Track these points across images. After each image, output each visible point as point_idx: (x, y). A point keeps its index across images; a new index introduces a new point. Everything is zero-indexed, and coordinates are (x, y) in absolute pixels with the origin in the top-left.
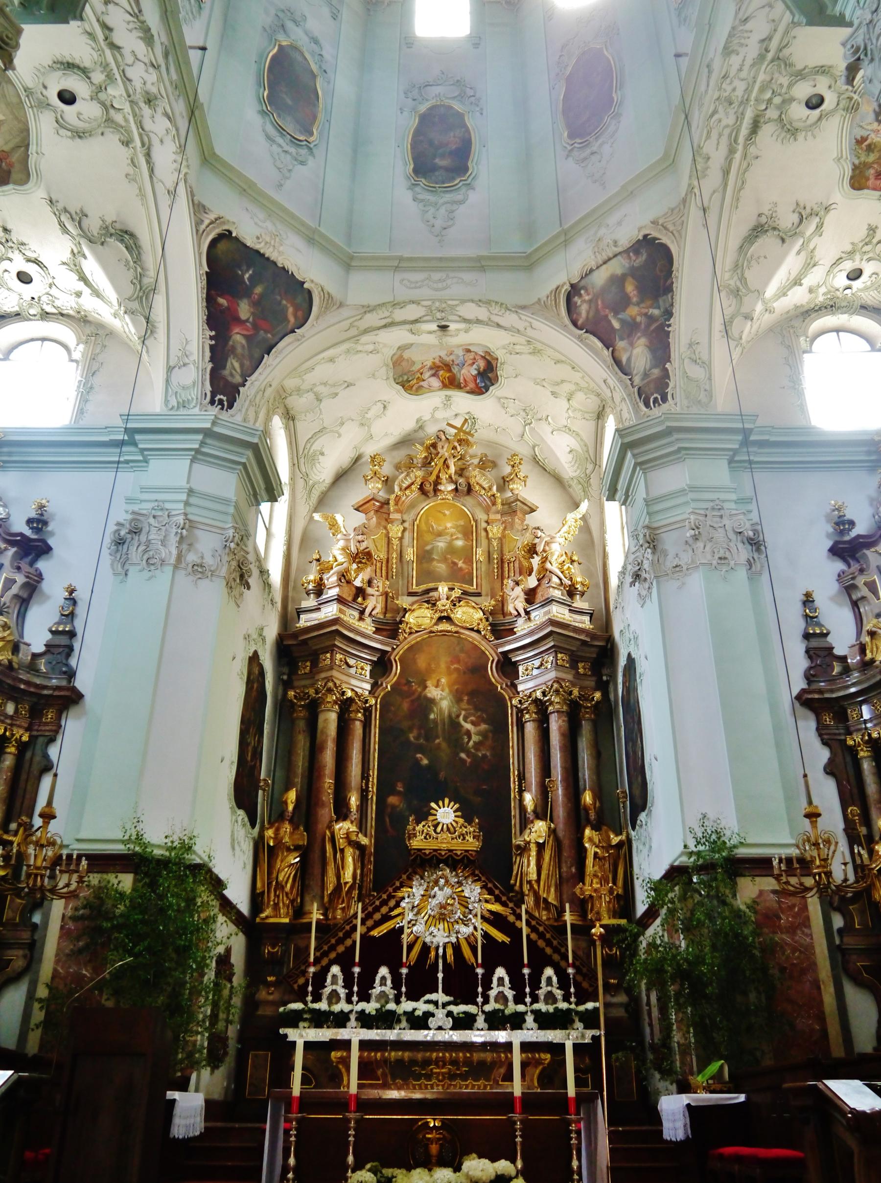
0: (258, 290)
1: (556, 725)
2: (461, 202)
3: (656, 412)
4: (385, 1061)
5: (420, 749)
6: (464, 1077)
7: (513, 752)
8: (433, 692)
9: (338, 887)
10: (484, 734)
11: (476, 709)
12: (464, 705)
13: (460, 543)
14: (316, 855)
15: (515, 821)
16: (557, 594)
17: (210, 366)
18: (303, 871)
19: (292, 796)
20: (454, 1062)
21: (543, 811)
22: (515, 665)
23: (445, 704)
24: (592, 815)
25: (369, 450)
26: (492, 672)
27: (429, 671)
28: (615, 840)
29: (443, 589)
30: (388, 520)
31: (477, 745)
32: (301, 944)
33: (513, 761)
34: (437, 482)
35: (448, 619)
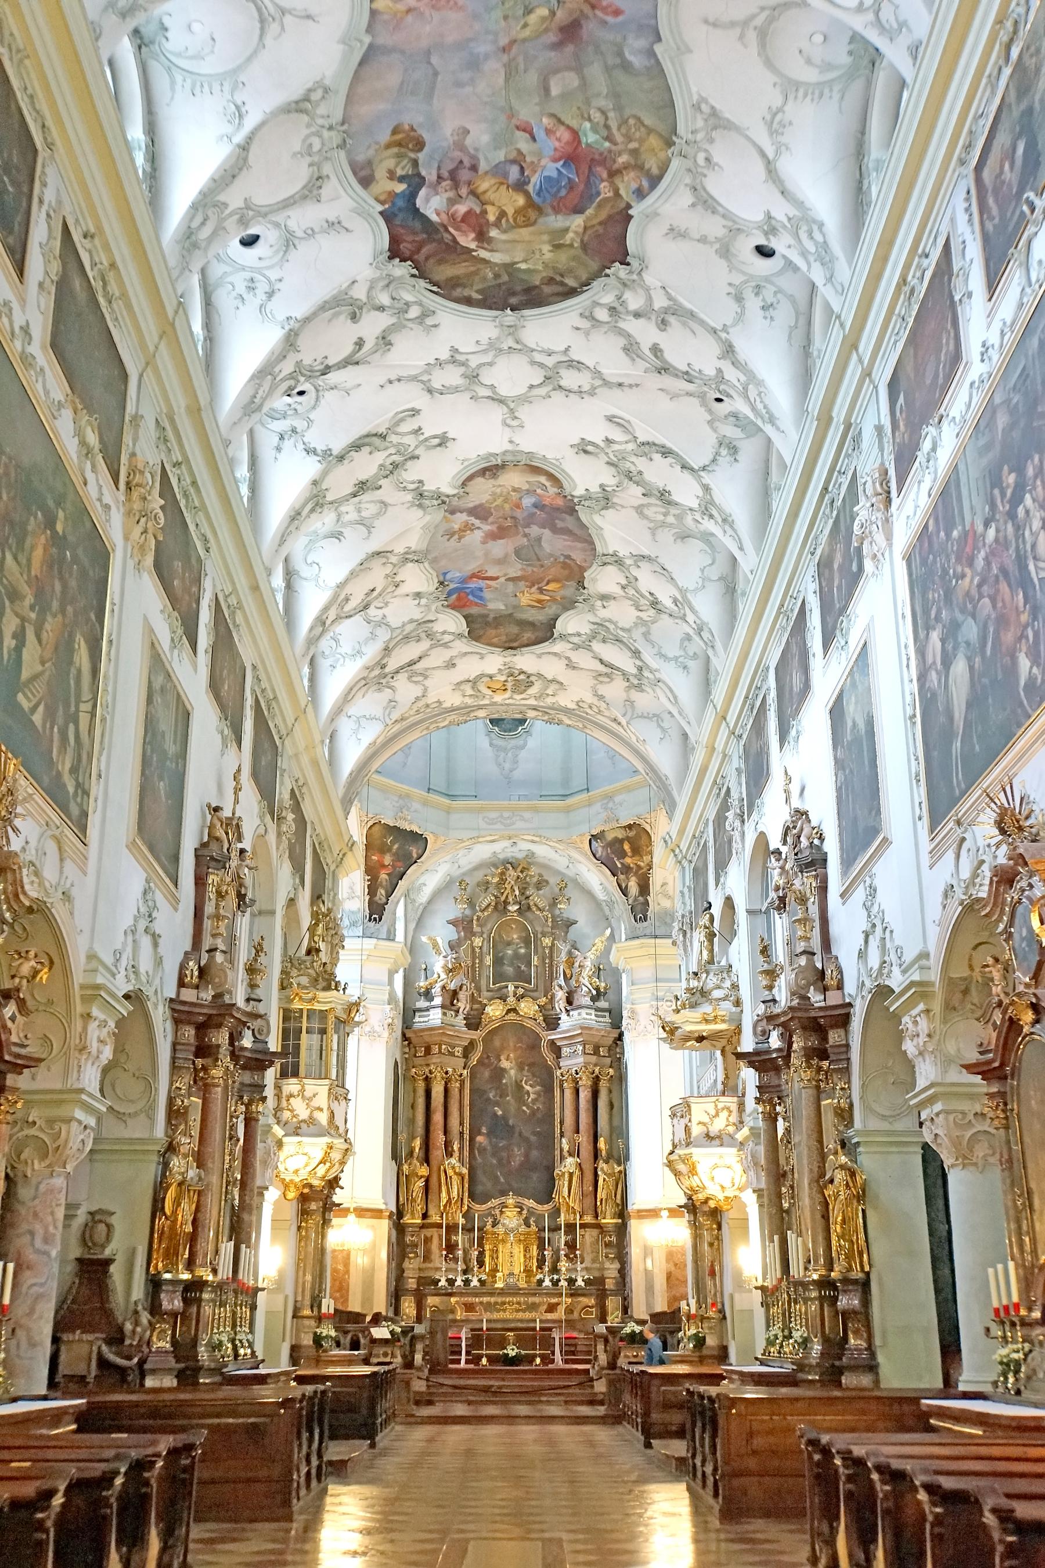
0: (396, 846)
1: (585, 1095)
2: (523, 747)
3: (640, 925)
4: (481, 1303)
5: (497, 1104)
6: (523, 1311)
7: (557, 1106)
8: (505, 1064)
9: (449, 1201)
10: (537, 1093)
11: (534, 1075)
12: (525, 1073)
13: (523, 951)
14: (434, 1181)
15: (558, 1158)
16: (587, 1001)
17: (367, 898)
18: (427, 1188)
19: (417, 1143)
20: (519, 1303)
21: (575, 1152)
22: (559, 1048)
23: (513, 1072)
24: (604, 1153)
25: (456, 873)
26: (545, 1051)
27: (503, 1048)
28: (617, 1169)
29: (511, 988)
30: (474, 934)
31: (534, 1101)
32: (429, 1235)
33: (557, 1111)
34: (506, 903)
35: (514, 1010)
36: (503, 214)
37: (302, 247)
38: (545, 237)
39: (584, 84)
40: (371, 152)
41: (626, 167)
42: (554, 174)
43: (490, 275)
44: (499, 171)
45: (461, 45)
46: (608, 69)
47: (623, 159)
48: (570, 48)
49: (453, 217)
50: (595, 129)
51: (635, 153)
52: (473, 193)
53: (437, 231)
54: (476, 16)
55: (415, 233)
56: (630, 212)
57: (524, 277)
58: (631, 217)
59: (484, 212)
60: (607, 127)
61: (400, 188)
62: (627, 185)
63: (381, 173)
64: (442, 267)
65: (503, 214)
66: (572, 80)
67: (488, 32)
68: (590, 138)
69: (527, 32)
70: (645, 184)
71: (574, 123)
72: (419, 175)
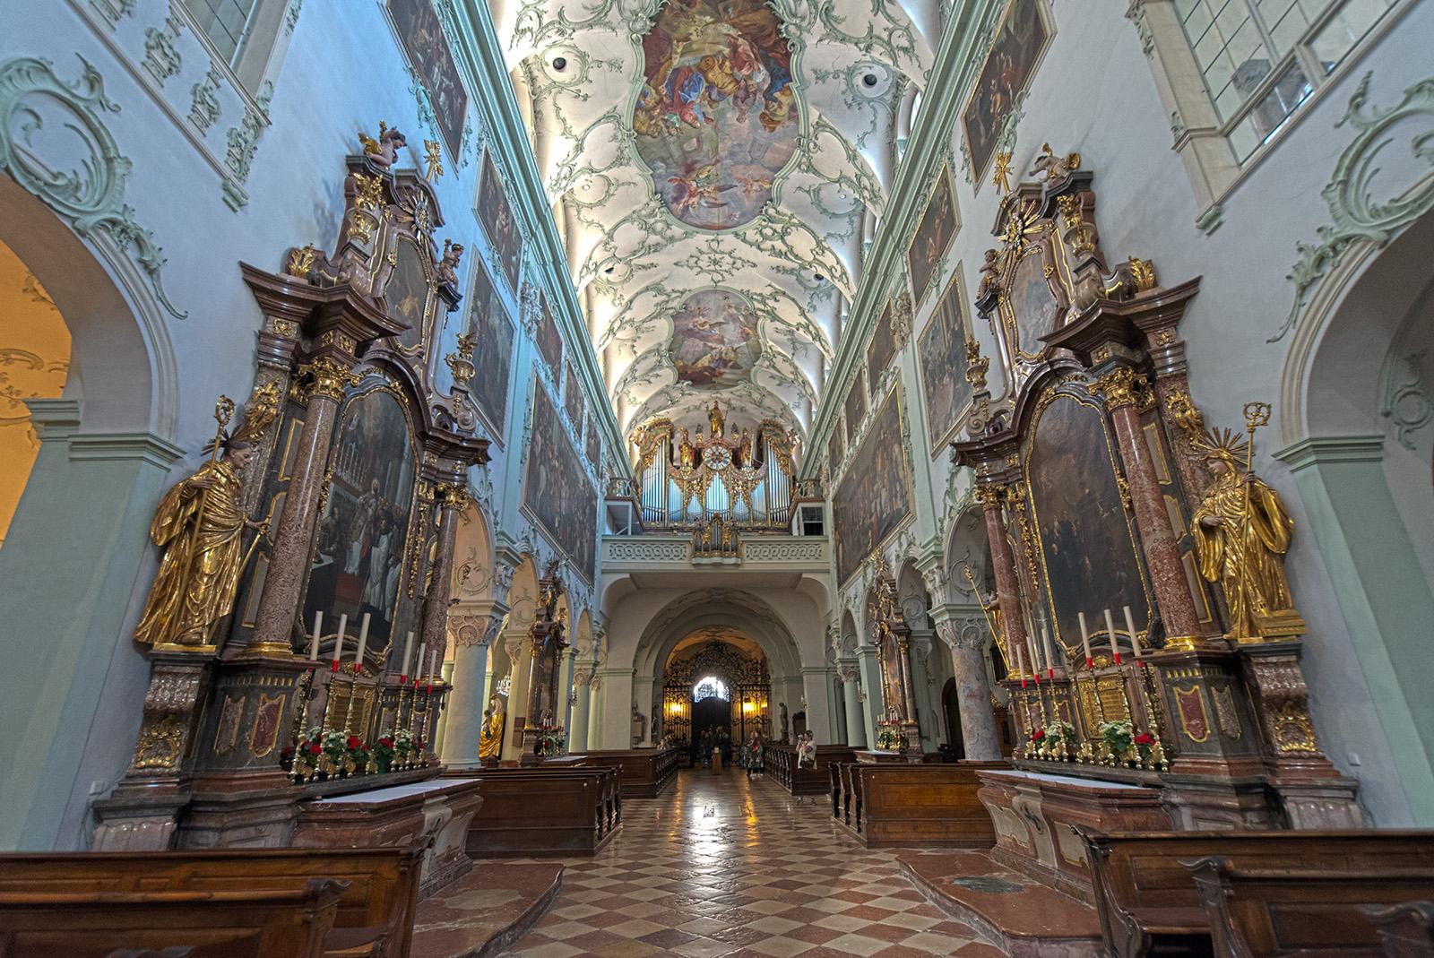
36: (721, 67)
37: (844, 67)
38: (695, 47)
39: (681, 145)
40: (787, 123)
41: (654, 108)
42: (692, 94)
43: (730, 10)
44: (722, 95)
45: (738, 163)
46: (672, 156)
47: (656, 113)
48: (689, 162)
49: (751, 66)
50: (674, 124)
51: (651, 118)
52: (738, 82)
53: (762, 56)
54: (730, 175)
55: (774, 58)
56: (645, 79)
57: (707, 7)
58: (646, 74)
59: (732, 69)
60: (667, 127)
61: (777, 95)
62: (650, 101)
63: (785, 109)
64: (763, 22)
65: (721, 67)
66: (687, 147)
67: (725, 169)
68: (674, 119)
69: (708, 168)
70: (643, 102)
71: (684, 125)
72: (766, 99)
